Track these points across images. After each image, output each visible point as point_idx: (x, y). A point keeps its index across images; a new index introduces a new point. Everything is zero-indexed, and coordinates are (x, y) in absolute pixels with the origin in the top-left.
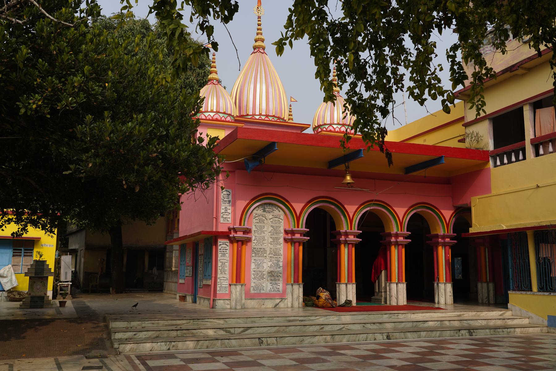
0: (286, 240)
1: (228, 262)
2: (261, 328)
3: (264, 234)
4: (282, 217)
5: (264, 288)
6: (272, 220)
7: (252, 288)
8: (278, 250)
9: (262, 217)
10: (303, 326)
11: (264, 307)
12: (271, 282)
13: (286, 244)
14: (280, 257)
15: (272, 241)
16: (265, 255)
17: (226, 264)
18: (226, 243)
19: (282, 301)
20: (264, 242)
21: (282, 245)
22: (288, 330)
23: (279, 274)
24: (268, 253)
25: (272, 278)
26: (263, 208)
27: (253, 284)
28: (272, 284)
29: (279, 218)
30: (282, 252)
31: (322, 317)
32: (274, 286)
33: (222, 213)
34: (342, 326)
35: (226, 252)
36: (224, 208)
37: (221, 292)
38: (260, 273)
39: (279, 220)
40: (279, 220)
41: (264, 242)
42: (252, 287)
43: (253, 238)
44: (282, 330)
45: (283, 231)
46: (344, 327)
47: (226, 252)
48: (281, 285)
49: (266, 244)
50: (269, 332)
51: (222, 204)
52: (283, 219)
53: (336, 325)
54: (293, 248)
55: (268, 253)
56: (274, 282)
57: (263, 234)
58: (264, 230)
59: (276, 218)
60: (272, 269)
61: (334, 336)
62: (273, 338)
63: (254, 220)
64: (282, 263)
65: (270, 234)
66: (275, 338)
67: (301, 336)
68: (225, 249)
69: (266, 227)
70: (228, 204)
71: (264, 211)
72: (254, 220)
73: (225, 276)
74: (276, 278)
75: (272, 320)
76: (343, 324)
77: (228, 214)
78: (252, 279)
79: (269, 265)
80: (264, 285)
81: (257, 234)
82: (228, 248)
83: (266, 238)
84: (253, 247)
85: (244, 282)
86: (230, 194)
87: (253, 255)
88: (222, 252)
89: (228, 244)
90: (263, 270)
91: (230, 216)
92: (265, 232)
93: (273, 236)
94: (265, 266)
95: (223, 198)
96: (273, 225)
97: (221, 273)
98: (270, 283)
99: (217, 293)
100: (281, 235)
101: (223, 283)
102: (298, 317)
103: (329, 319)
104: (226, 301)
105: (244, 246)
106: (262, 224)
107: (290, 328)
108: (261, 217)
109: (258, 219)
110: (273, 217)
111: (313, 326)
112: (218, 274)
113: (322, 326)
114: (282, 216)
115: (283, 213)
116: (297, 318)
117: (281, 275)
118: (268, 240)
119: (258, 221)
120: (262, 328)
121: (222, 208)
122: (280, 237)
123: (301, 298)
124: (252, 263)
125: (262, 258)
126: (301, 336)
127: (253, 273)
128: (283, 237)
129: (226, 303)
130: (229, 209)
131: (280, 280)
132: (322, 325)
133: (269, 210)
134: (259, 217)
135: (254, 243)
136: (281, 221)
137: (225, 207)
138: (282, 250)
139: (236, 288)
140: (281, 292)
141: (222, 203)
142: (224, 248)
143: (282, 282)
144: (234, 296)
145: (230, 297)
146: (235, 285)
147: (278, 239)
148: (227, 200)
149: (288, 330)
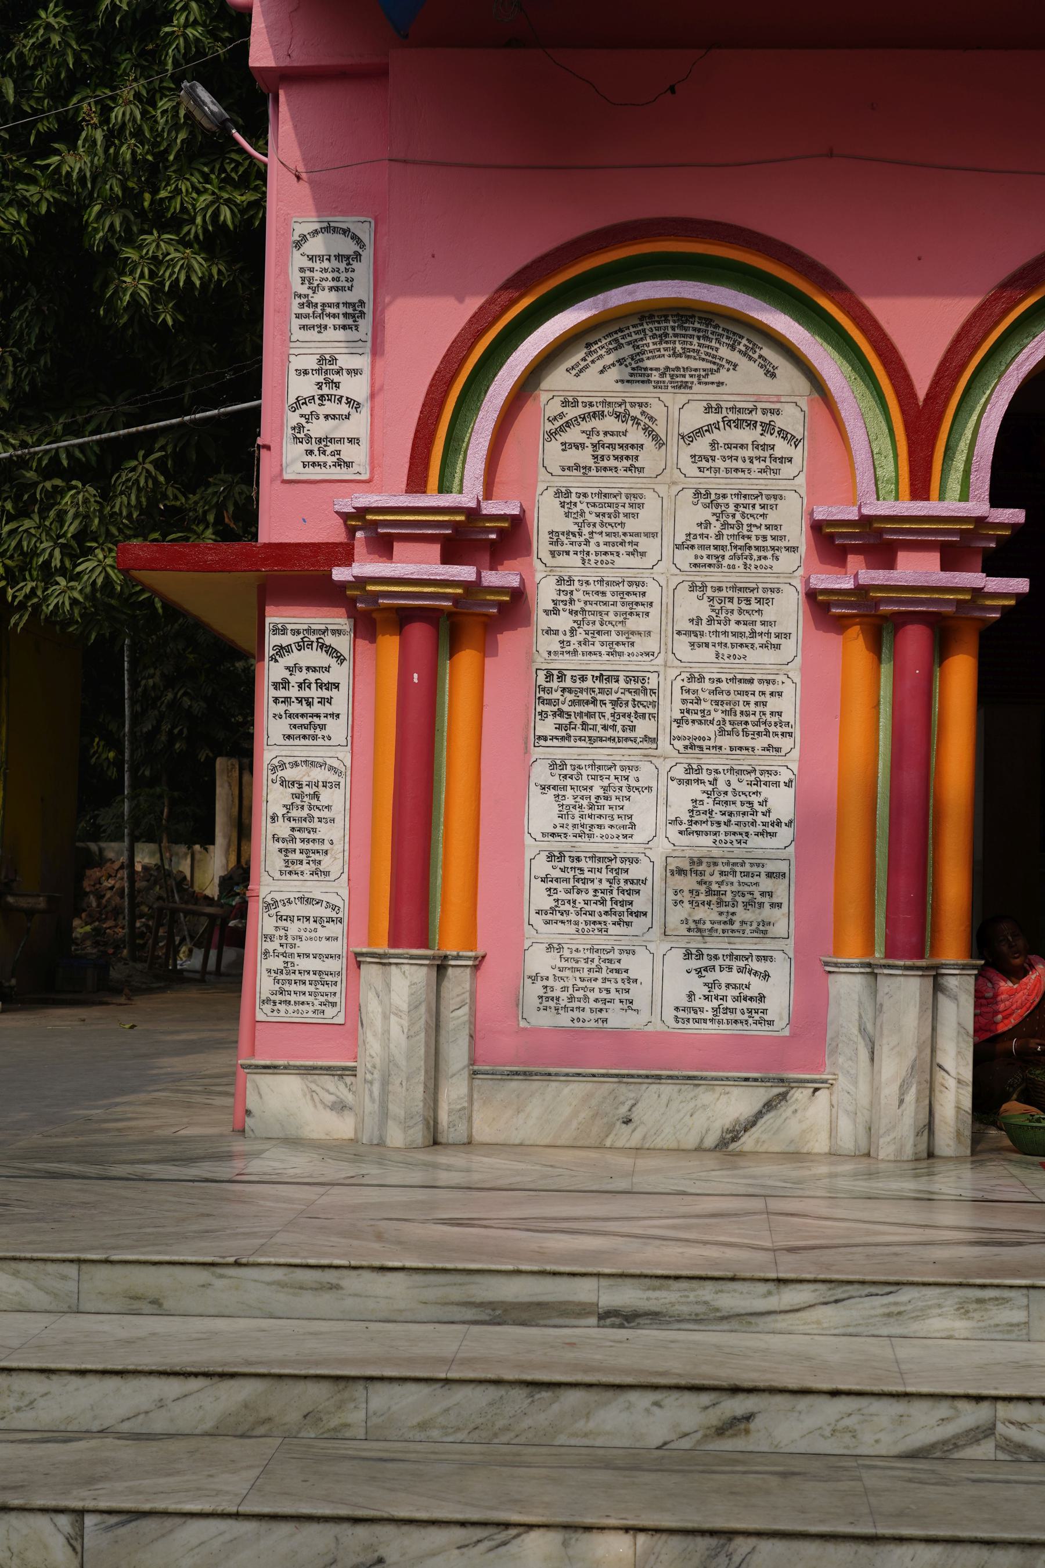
0: (826, 607)
1: (345, 781)
2: (76, 1381)
3: (634, 561)
4: (791, 419)
5: (639, 994)
6: (701, 446)
7: (532, 991)
8: (756, 687)
9: (617, 426)
10: (518, 1395)
11: (635, 1140)
12: (694, 945)
13: (831, 641)
14: (776, 742)
15: (705, 612)
16: (644, 728)
17: (326, 796)
18: (329, 640)
19: (783, 1097)
20: (633, 623)
21: (790, 647)
22: (356, 1416)
23: (766, 884)
24: (670, 707)
25: (701, 913)
26: (627, 351)
27: (540, 961)
28: (705, 962)
29: (768, 428)
30: (788, 705)
31: (839, 1292)
32: (724, 977)
33: (300, 402)
34: (972, 1416)
35: (327, 709)
36: (311, 363)
37: (285, 1014)
38: (605, 875)
39: (768, 439)
40: (768, 439)
41: (633, 623)
42: (534, 978)
43: (545, 593)
44: (293, 1417)
45: (797, 534)
46: (988, 1431)
47: (327, 709)
48: (780, 971)
49: (651, 644)
50: (159, 1424)
51: (298, 334)
52: (798, 431)
53: (898, 1407)
54: (886, 670)
55: (670, 707)
56: (716, 945)
57: (624, 561)
58: (631, 525)
59: (739, 424)
60: (708, 841)
61: (742, 1546)
62: (42, 1522)
63: (554, 446)
64: (791, 791)
65: (685, 558)
66: (63, 1521)
67: (356, 1521)
68: (320, 685)
69: (651, 502)
70: (341, 334)
71: (638, 375)
72: (553, 453)
73: (316, 889)
74: (741, 914)
75: (327, 1297)
76: (979, 1399)
77: (343, 409)
78: (537, 920)
79: (680, 807)
80: (638, 965)
81: (577, 560)
82: (340, 673)
83: (653, 593)
84: (541, 661)
85: (472, 945)
86: (357, 256)
87: (547, 727)
88: (295, 708)
89: (343, 644)
90: (626, 848)
91: (359, 425)
92: (644, 543)
93: (714, 577)
94: (641, 808)
95: (304, 290)
96: (716, 484)
97: (290, 869)
98: (688, 955)
99: (260, 1016)
100: (778, 567)
101: (304, 947)
102: (590, 1284)
103: (921, 1314)
104: (329, 1082)
105: (467, 658)
106: (621, 482)
107: (381, 1398)
108: (610, 423)
109: (582, 439)
110: (713, 418)
111: (633, 1396)
112: (265, 878)
113: (738, 1405)
114: (789, 410)
115: (802, 384)
116: (584, 1291)
117: (781, 890)
118: (669, 610)
119: (585, 457)
120: (90, 1379)
121: (297, 363)
122: (770, 581)
123: (951, 1083)
124: (534, 790)
125: (622, 756)
126: (356, 1521)
127: (542, 867)
128: (798, 583)
129: (330, 1099)
130: (355, 372)
131: (773, 931)
132: (735, 1390)
133: (682, 362)
134: (595, 423)
135: (549, 631)
136: (782, 448)
137: (322, 360)
138: (788, 689)
139: (388, 985)
140: (781, 1026)
141: (296, 323)
142: (312, 677)
143: (790, 946)
144: (373, 1046)
145: (355, 1059)
146: (382, 960)
147: (767, 596)
148: (332, 297)
149: (356, 1416)
